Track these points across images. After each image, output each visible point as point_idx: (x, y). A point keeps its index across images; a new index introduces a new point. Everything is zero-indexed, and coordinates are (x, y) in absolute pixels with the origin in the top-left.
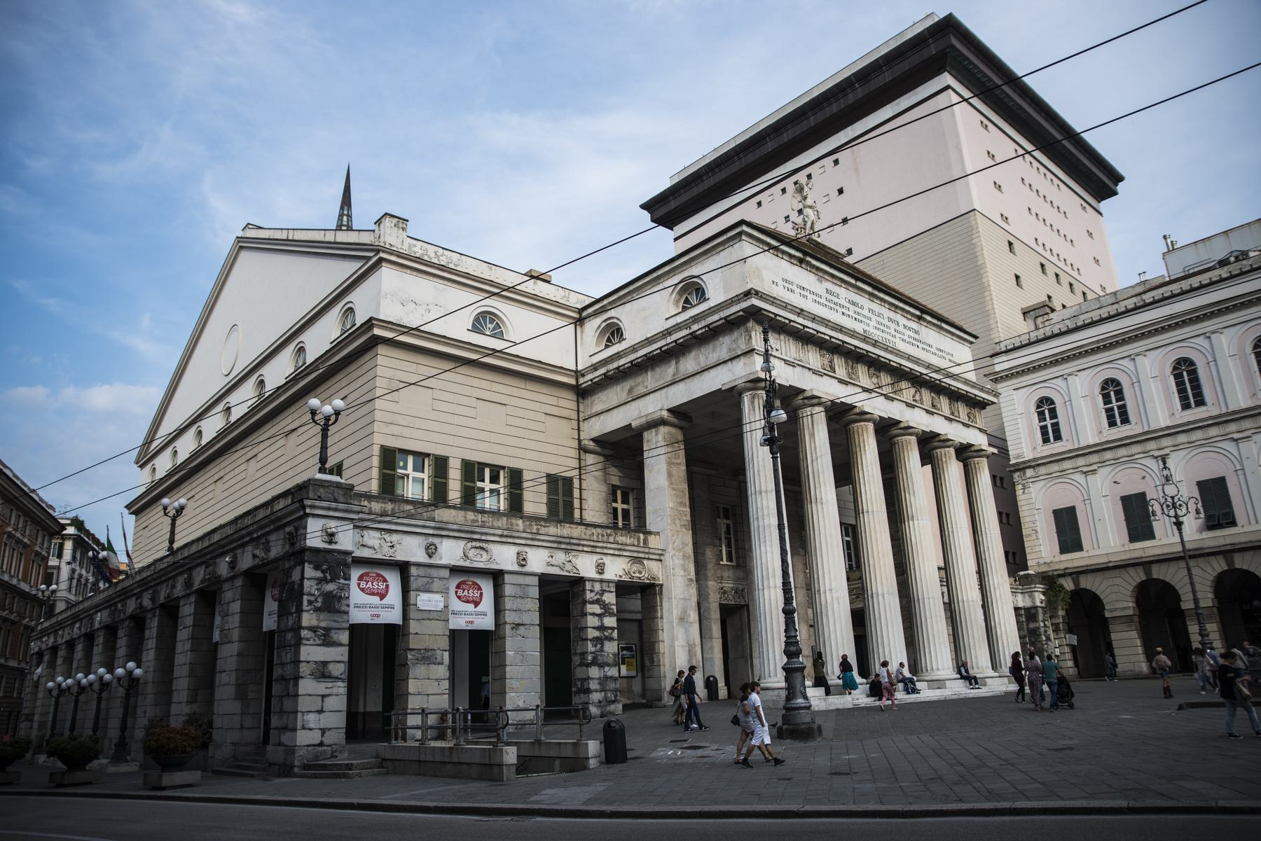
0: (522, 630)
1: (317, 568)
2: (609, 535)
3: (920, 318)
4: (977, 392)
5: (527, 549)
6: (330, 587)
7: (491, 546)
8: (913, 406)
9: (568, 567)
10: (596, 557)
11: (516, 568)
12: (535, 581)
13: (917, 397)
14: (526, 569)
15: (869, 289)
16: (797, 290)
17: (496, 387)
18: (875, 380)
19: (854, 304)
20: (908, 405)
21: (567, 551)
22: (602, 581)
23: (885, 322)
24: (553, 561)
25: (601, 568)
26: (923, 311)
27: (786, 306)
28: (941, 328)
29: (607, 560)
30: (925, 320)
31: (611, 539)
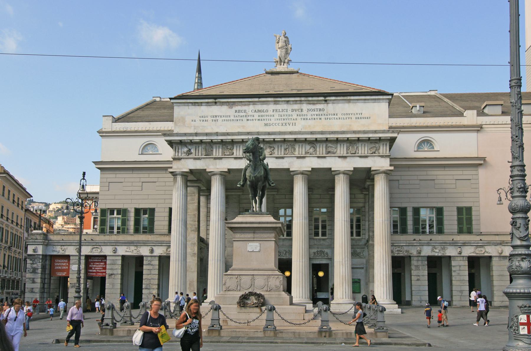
0: (113, 276)
1: (31, 260)
3: (326, 101)
4: (370, 135)
5: (116, 247)
6: (35, 266)
8: (304, 157)
9: (135, 252)
10: (149, 248)
11: (112, 254)
12: (120, 258)
13: (311, 150)
15: (272, 99)
16: (210, 119)
17: (151, 175)
19: (259, 111)
20: (298, 158)
21: (135, 246)
22: (151, 256)
23: (290, 112)
24: (128, 250)
25: (152, 251)
26: (325, 97)
27: (185, 135)
29: (154, 248)
30: (330, 100)
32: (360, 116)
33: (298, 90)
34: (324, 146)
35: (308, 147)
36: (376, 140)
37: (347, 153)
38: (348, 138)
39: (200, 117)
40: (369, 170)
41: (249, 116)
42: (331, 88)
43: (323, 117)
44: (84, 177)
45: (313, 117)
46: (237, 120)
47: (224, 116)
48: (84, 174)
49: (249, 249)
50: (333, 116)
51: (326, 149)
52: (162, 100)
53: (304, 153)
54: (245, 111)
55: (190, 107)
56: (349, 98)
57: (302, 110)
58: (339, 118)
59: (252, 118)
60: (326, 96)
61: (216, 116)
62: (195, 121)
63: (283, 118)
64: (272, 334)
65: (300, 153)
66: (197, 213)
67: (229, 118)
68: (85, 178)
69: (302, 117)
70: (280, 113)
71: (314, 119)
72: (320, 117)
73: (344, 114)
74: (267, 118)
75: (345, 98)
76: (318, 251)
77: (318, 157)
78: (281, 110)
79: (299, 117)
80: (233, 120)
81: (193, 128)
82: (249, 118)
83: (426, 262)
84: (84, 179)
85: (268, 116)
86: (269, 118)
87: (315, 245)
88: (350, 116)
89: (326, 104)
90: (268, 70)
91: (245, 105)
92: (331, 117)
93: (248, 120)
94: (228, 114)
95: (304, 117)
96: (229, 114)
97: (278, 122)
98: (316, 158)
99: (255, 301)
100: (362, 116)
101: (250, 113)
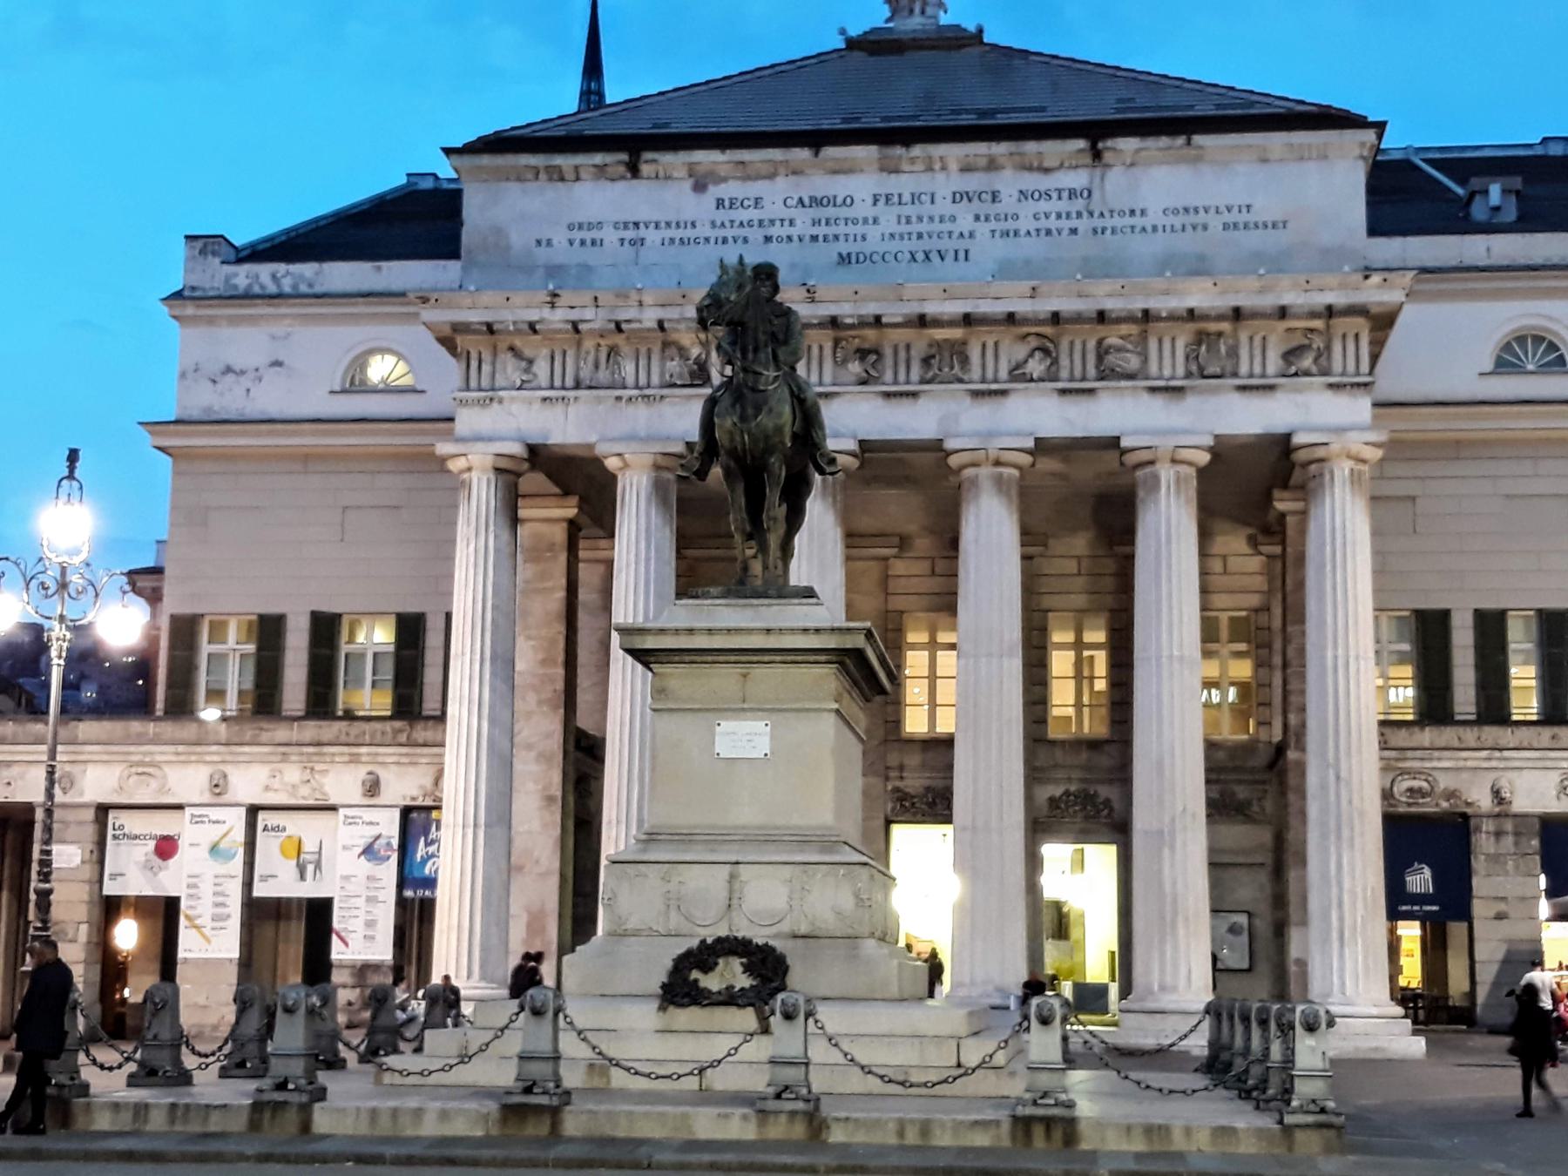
2: (397, 732)
3: (1097, 155)
5: (228, 769)
7: (166, 769)
8: (1004, 393)
11: (207, 798)
13: (1036, 367)
14: (225, 799)
16: (610, 236)
18: (855, 367)
19: (816, 202)
20: (976, 394)
23: (944, 206)
24: (276, 784)
25: (373, 787)
28: (1201, 147)
31: (403, 738)
32: (1243, 217)
33: (983, 114)
34: (1092, 344)
35: (1021, 351)
36: (1313, 315)
37: (1189, 375)
38: (1191, 311)
39: (570, 227)
40: (1282, 445)
41: (772, 222)
42: (1119, 101)
43: (1083, 224)
44: (72, 468)
45: (1043, 224)
46: (725, 241)
47: (668, 224)
48: (73, 456)
49: (724, 748)
50: (1128, 221)
51: (1100, 358)
52: (446, 186)
53: (1003, 373)
54: (757, 201)
55: (528, 184)
56: (1198, 139)
57: (995, 196)
58: (1155, 228)
59: (786, 231)
60: (1096, 133)
61: (636, 225)
62: (549, 243)
63: (916, 227)
64: (799, 1131)
65: (990, 374)
66: (561, 628)
67: (689, 233)
68: (77, 474)
69: (993, 225)
70: (908, 210)
71: (1049, 232)
72: (1074, 223)
73: (1176, 212)
74: (851, 229)
75: (1181, 140)
76: (1067, 793)
77: (1063, 392)
78: (907, 198)
79: (983, 229)
80: (707, 240)
81: (540, 272)
82: (776, 231)
83: (1535, 843)
84: (71, 476)
85: (855, 222)
86: (859, 229)
87: (1056, 766)
88: (1201, 218)
89: (1098, 172)
90: (854, 31)
91: (758, 177)
92: (1117, 221)
93: (768, 239)
94: (688, 216)
95: (1003, 226)
96: (690, 220)
97: (893, 246)
98: (1055, 395)
99: (743, 981)
100: (1251, 218)
101: (778, 211)
